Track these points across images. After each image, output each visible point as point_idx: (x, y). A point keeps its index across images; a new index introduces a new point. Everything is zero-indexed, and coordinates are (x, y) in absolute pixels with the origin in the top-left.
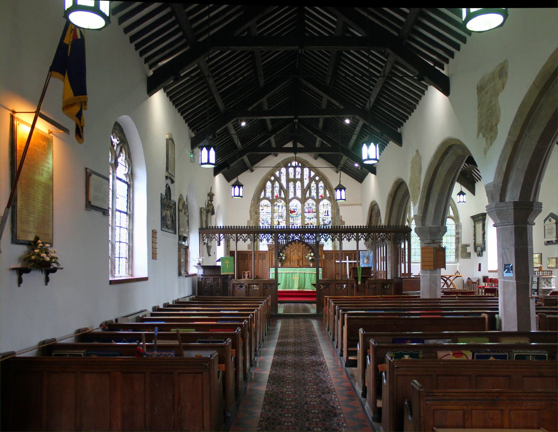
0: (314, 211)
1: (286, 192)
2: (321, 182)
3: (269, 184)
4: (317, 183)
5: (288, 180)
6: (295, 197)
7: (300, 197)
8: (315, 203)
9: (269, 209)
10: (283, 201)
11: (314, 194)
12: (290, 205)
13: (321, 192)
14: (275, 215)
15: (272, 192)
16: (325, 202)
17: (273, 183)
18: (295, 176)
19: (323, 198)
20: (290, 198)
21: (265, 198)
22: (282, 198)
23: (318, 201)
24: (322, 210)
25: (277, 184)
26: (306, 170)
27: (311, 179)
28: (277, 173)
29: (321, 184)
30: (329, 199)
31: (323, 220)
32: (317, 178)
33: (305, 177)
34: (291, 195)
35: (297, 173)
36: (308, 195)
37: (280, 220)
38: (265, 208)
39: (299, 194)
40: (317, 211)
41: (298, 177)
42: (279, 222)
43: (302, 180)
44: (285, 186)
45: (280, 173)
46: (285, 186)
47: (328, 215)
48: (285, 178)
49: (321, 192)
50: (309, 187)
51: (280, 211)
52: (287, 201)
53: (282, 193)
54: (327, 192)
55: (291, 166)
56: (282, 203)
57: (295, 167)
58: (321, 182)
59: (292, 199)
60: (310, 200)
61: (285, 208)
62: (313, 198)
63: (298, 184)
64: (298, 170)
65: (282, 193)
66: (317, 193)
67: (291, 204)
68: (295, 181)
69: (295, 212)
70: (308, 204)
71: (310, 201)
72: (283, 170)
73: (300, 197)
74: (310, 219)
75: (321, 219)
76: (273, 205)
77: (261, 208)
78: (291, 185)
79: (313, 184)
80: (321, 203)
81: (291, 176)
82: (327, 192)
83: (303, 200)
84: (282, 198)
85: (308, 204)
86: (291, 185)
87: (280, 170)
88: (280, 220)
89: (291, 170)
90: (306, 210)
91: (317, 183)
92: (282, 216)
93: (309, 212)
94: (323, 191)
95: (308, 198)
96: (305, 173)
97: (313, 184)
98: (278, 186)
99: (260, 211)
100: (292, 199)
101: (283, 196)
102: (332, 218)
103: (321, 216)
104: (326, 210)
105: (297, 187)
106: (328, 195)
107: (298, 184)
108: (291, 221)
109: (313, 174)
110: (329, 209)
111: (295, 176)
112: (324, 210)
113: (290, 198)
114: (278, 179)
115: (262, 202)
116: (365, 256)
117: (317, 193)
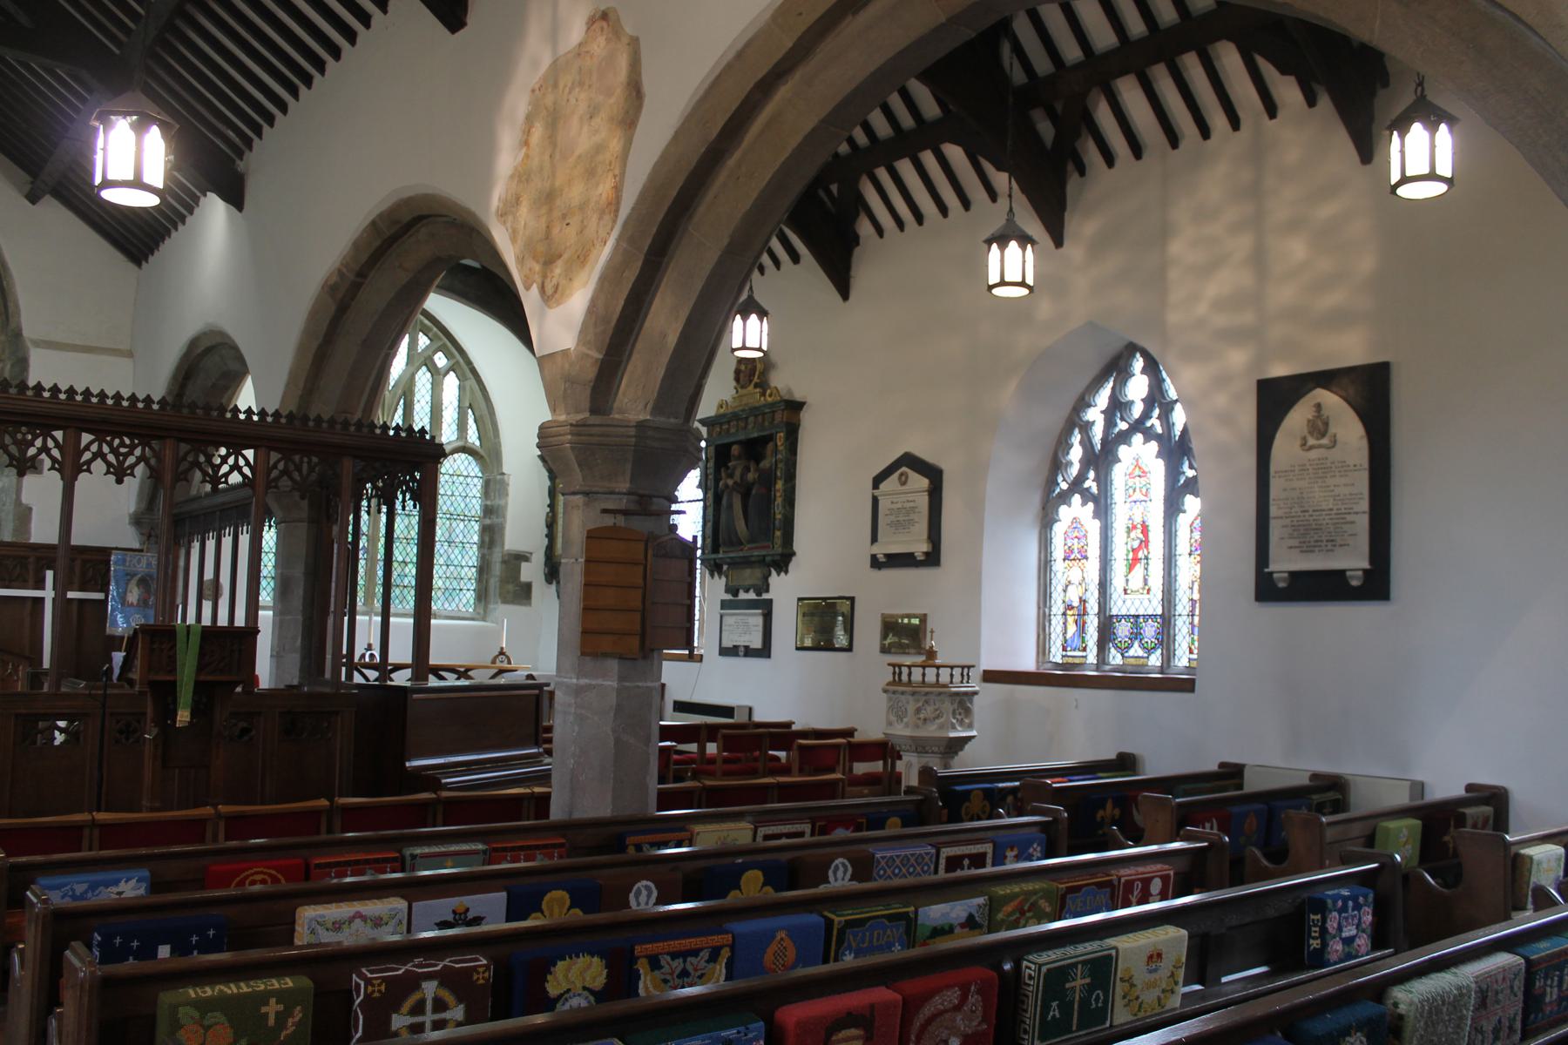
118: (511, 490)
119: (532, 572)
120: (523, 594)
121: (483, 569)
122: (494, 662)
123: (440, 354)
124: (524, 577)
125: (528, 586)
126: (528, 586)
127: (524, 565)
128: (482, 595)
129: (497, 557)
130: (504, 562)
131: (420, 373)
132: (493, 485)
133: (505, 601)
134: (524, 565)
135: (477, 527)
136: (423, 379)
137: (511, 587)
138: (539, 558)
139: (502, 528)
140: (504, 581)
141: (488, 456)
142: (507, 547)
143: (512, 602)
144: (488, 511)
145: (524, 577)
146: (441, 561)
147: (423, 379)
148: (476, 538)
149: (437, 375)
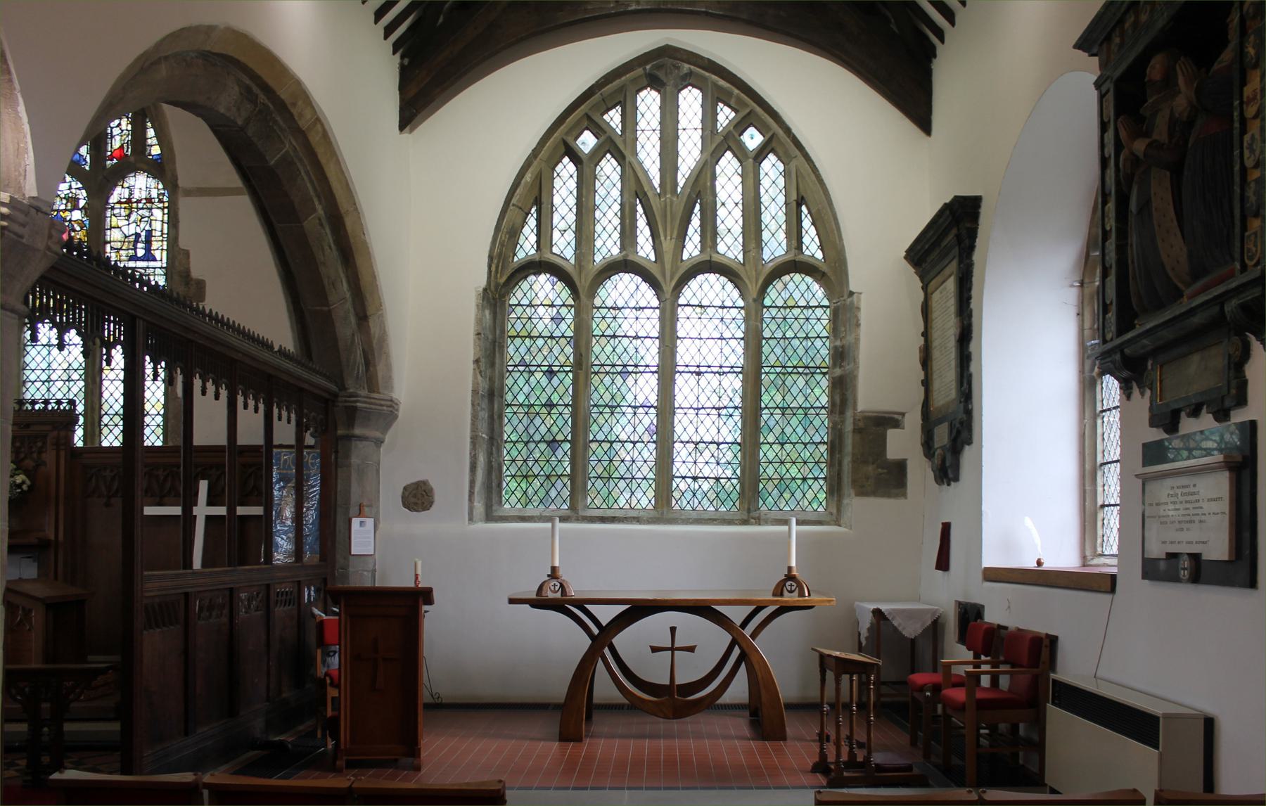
16: (141, 184)
47: (149, 256)
80: (118, 194)
112: (132, 229)
118: (863, 316)
119: (902, 444)
120: (893, 479)
121: (835, 446)
122: (779, 591)
123: (752, 130)
124: (893, 453)
125: (900, 468)
126: (900, 468)
127: (891, 434)
128: (834, 488)
129: (849, 427)
130: (857, 431)
131: (723, 162)
132: (843, 314)
133: (862, 492)
134: (891, 434)
135: (825, 383)
136: (728, 166)
137: (870, 469)
138: (913, 421)
139: (854, 378)
140: (859, 461)
141: (830, 272)
142: (861, 406)
143: (874, 493)
144: (841, 355)
145: (893, 453)
146: (771, 439)
147: (728, 166)
148: (824, 400)
149: (751, 162)
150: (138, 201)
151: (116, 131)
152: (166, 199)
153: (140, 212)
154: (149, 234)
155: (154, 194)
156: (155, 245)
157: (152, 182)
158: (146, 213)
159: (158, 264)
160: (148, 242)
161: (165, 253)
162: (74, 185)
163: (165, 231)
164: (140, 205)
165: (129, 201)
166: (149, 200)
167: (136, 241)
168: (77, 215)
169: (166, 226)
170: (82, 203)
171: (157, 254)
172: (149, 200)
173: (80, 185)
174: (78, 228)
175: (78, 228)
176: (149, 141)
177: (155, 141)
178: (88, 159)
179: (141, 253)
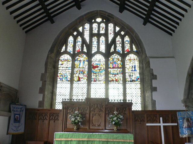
0: (120, 66)
1: (89, 47)
2: (127, 36)
3: (71, 39)
4: (123, 37)
5: (92, 35)
6: (98, 52)
7: (104, 51)
8: (120, 58)
9: (70, 64)
10: (85, 56)
11: (119, 48)
12: (92, 60)
13: (127, 47)
14: (76, 70)
15: (74, 47)
16: (132, 56)
17: (75, 38)
18: (99, 31)
19: (129, 53)
20: (93, 52)
21: (66, 52)
22: (84, 53)
23: (123, 56)
24: (128, 65)
25: (79, 39)
26: (111, 26)
27: (116, 34)
28: (81, 29)
29: (127, 39)
30: (137, 53)
31: (130, 76)
32: (123, 33)
33: (109, 32)
34: (94, 50)
35: (101, 29)
36: (112, 50)
37: (81, 76)
38: (65, 63)
39: (103, 48)
40: (123, 67)
41: (102, 32)
42: (79, 78)
43: (106, 35)
44: (88, 41)
45: (83, 29)
46: (88, 41)
47: (135, 70)
48: (88, 34)
49: (127, 47)
50: (114, 41)
51: (81, 66)
52: (90, 55)
53: (85, 47)
54: (134, 46)
55: (95, 22)
56: (84, 57)
57: (99, 24)
58: (127, 36)
59: (96, 53)
60: (115, 55)
61: (86, 63)
62: (118, 53)
63: (102, 39)
64: (103, 25)
65: (85, 47)
66: (123, 47)
67: (93, 59)
68: (99, 35)
69: (98, 67)
70: (113, 59)
71: (116, 57)
72: (87, 26)
73: (104, 51)
74: (115, 75)
75: (127, 75)
76: (74, 60)
77: (60, 63)
78: (95, 39)
79: (118, 39)
80: (127, 58)
81: (95, 31)
82: (134, 46)
83: (107, 55)
84: (84, 53)
85: (113, 59)
86: (95, 39)
87: (83, 26)
88: (81, 76)
89: (95, 26)
90: (111, 66)
91: (123, 37)
92: (83, 72)
93: (113, 68)
94: (129, 45)
95: (113, 53)
96: (109, 28)
97: (118, 39)
98: (81, 41)
99: (59, 66)
100: (96, 53)
101: (85, 50)
102: (140, 74)
103: (127, 71)
104: (133, 65)
105: (101, 41)
106: (135, 50)
107: (102, 39)
108: (93, 77)
109: (118, 29)
110: (137, 63)
111: (99, 31)
112: (131, 65)
113: (93, 52)
114: (81, 34)
115: (62, 56)
116: (184, 118)
117: (123, 47)
150: (132, 60)
151: (126, 46)
152: (138, 59)
153: (133, 62)
154: (135, 66)
155: (135, 58)
156: (136, 68)
157: (135, 56)
158: (134, 62)
159: (137, 72)
160: (135, 67)
161: (139, 70)
162: (118, 56)
163: (138, 65)
164: (132, 60)
165: (130, 59)
166: (134, 59)
167: (132, 67)
168: (119, 62)
169: (138, 64)
170: (120, 60)
171: (137, 70)
172: (134, 59)
173: (119, 56)
174: (119, 65)
175: (119, 65)
176: (133, 48)
177: (135, 48)
178: (121, 51)
179: (133, 70)
